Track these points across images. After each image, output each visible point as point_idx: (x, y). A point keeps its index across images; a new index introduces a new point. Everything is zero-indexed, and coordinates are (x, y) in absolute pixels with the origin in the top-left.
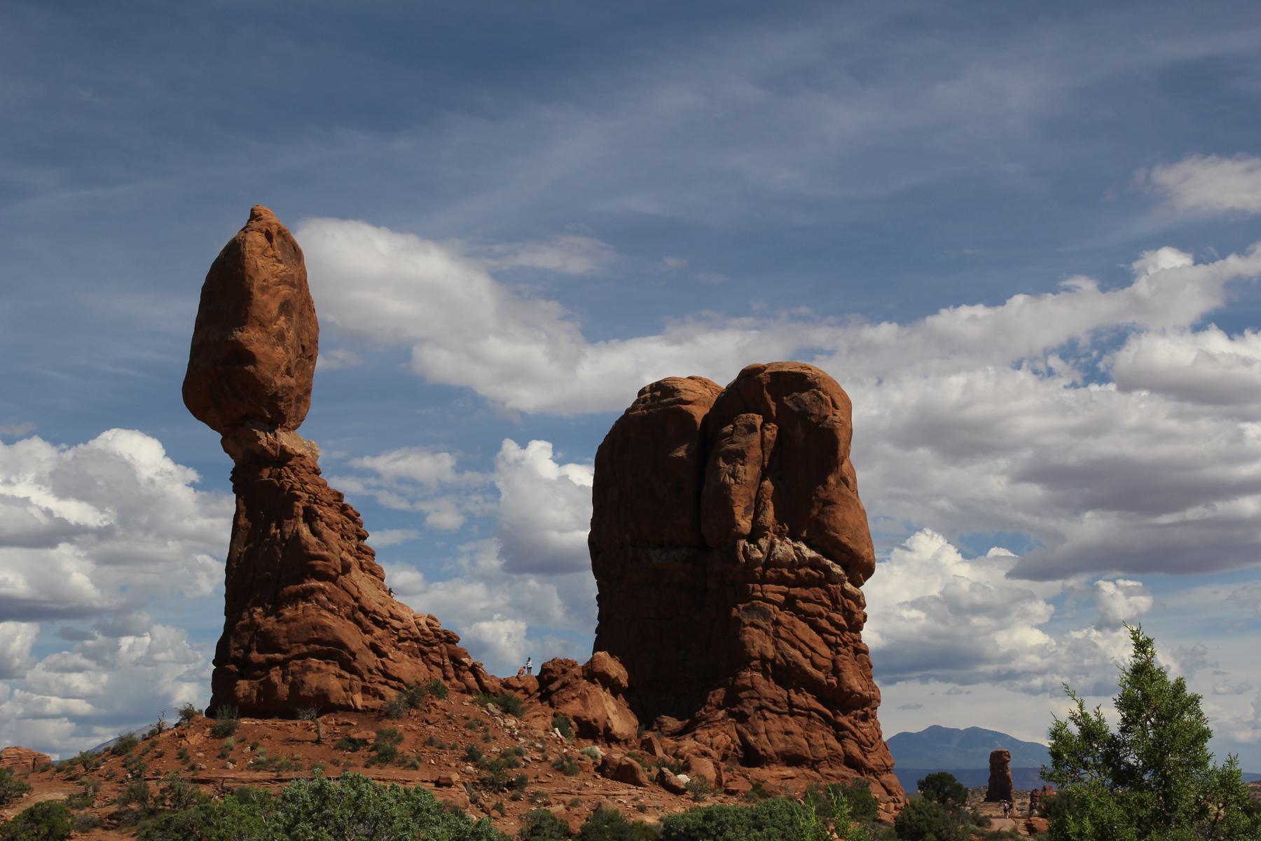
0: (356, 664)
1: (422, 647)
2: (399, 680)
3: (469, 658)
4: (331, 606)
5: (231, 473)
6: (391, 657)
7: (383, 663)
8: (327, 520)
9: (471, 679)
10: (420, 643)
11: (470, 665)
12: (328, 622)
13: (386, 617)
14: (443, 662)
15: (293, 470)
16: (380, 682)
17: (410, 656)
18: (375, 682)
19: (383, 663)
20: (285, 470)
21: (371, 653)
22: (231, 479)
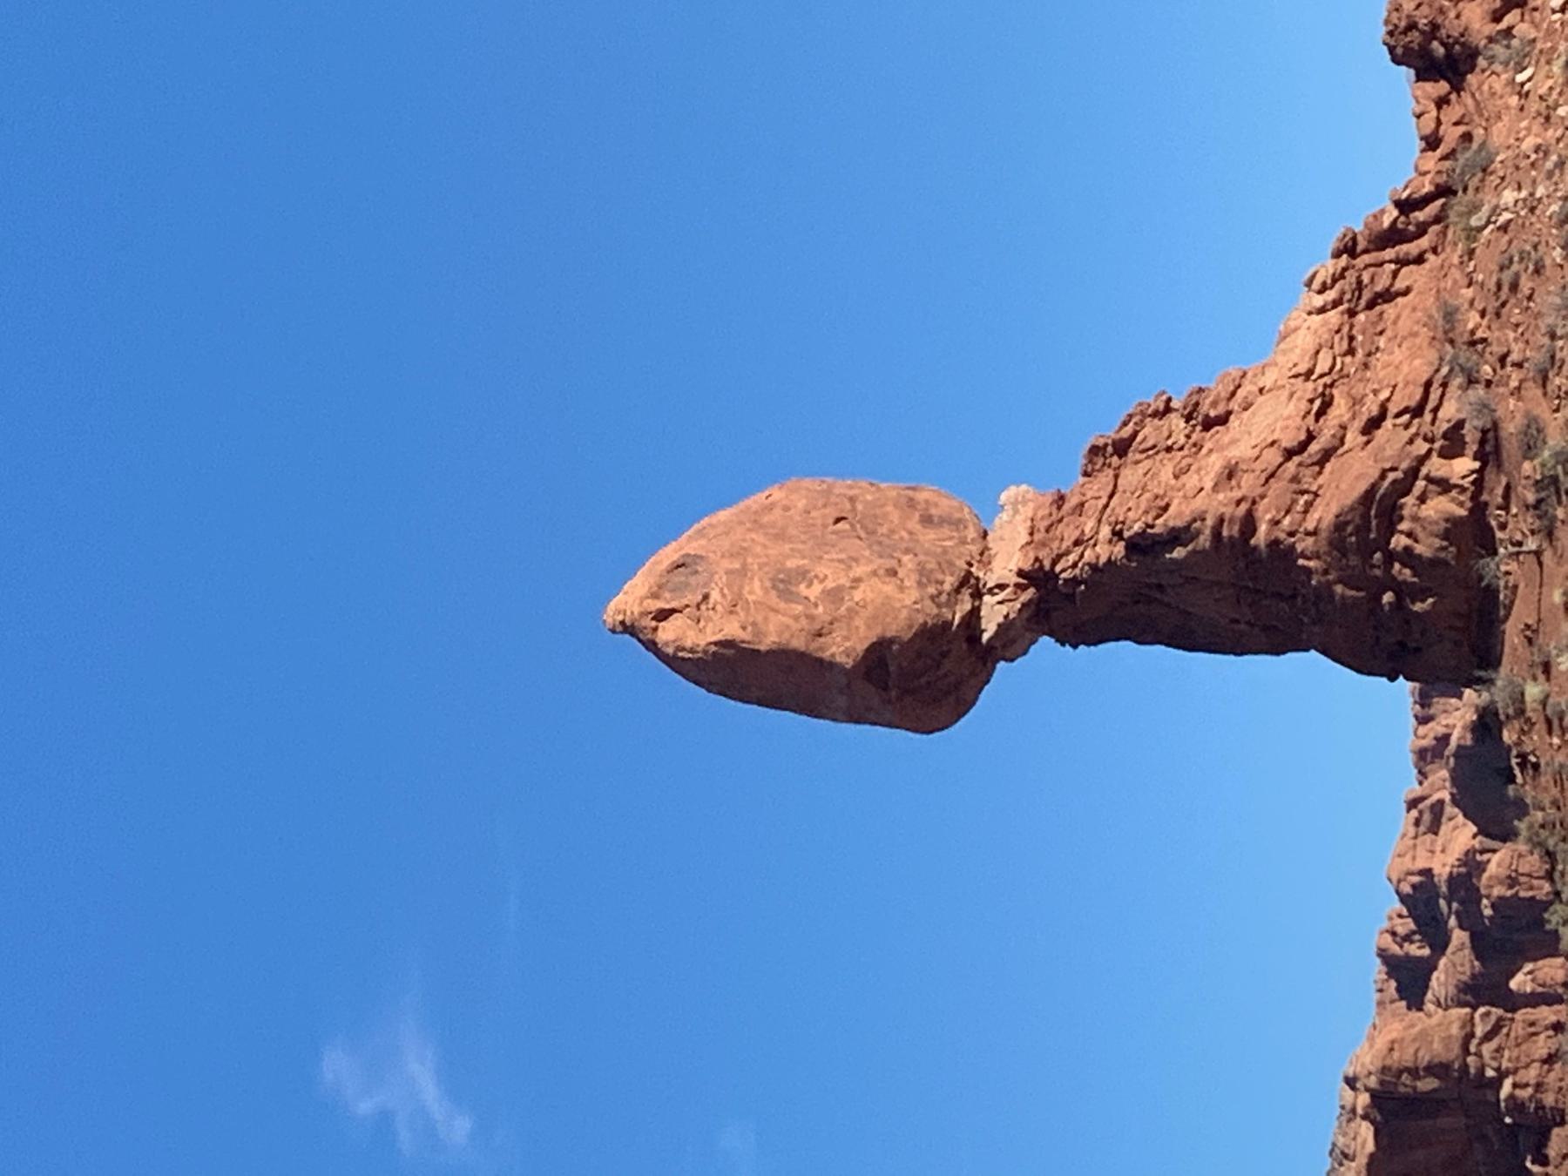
0: (1404, 465)
1: (1363, 302)
2: (1428, 385)
3: (1383, 212)
4: (1299, 507)
5: (1063, 644)
6: (1384, 395)
7: (1398, 415)
8: (1153, 513)
9: (1420, 216)
10: (1357, 306)
11: (1395, 213)
12: (1329, 519)
13: (1315, 389)
14: (1390, 261)
15: (1059, 557)
16: (1433, 422)
17: (1381, 333)
18: (1432, 432)
19: (1398, 415)
20: (1063, 570)
21: (1380, 434)
22: (1075, 646)
